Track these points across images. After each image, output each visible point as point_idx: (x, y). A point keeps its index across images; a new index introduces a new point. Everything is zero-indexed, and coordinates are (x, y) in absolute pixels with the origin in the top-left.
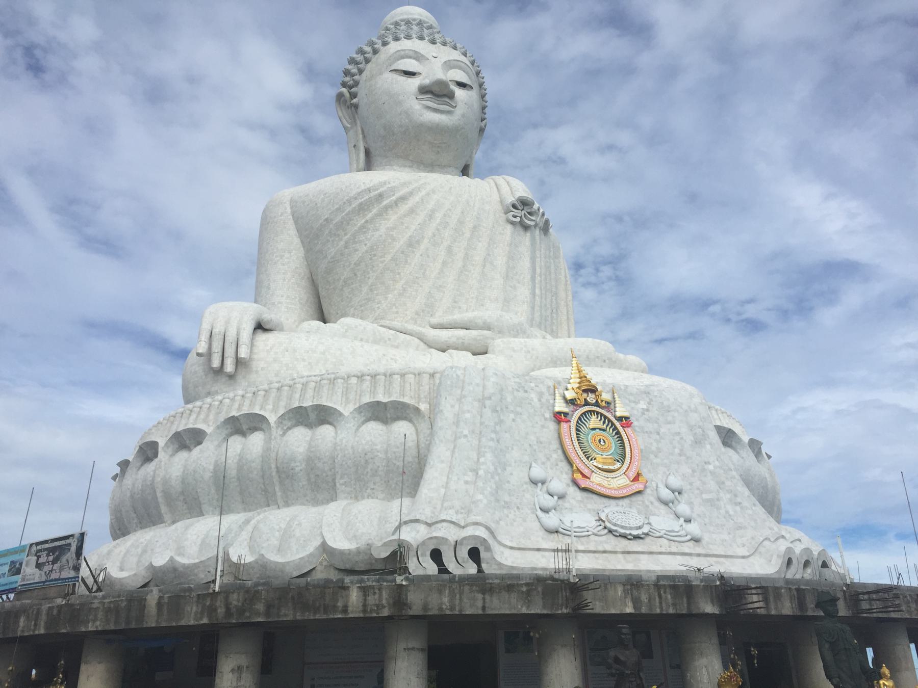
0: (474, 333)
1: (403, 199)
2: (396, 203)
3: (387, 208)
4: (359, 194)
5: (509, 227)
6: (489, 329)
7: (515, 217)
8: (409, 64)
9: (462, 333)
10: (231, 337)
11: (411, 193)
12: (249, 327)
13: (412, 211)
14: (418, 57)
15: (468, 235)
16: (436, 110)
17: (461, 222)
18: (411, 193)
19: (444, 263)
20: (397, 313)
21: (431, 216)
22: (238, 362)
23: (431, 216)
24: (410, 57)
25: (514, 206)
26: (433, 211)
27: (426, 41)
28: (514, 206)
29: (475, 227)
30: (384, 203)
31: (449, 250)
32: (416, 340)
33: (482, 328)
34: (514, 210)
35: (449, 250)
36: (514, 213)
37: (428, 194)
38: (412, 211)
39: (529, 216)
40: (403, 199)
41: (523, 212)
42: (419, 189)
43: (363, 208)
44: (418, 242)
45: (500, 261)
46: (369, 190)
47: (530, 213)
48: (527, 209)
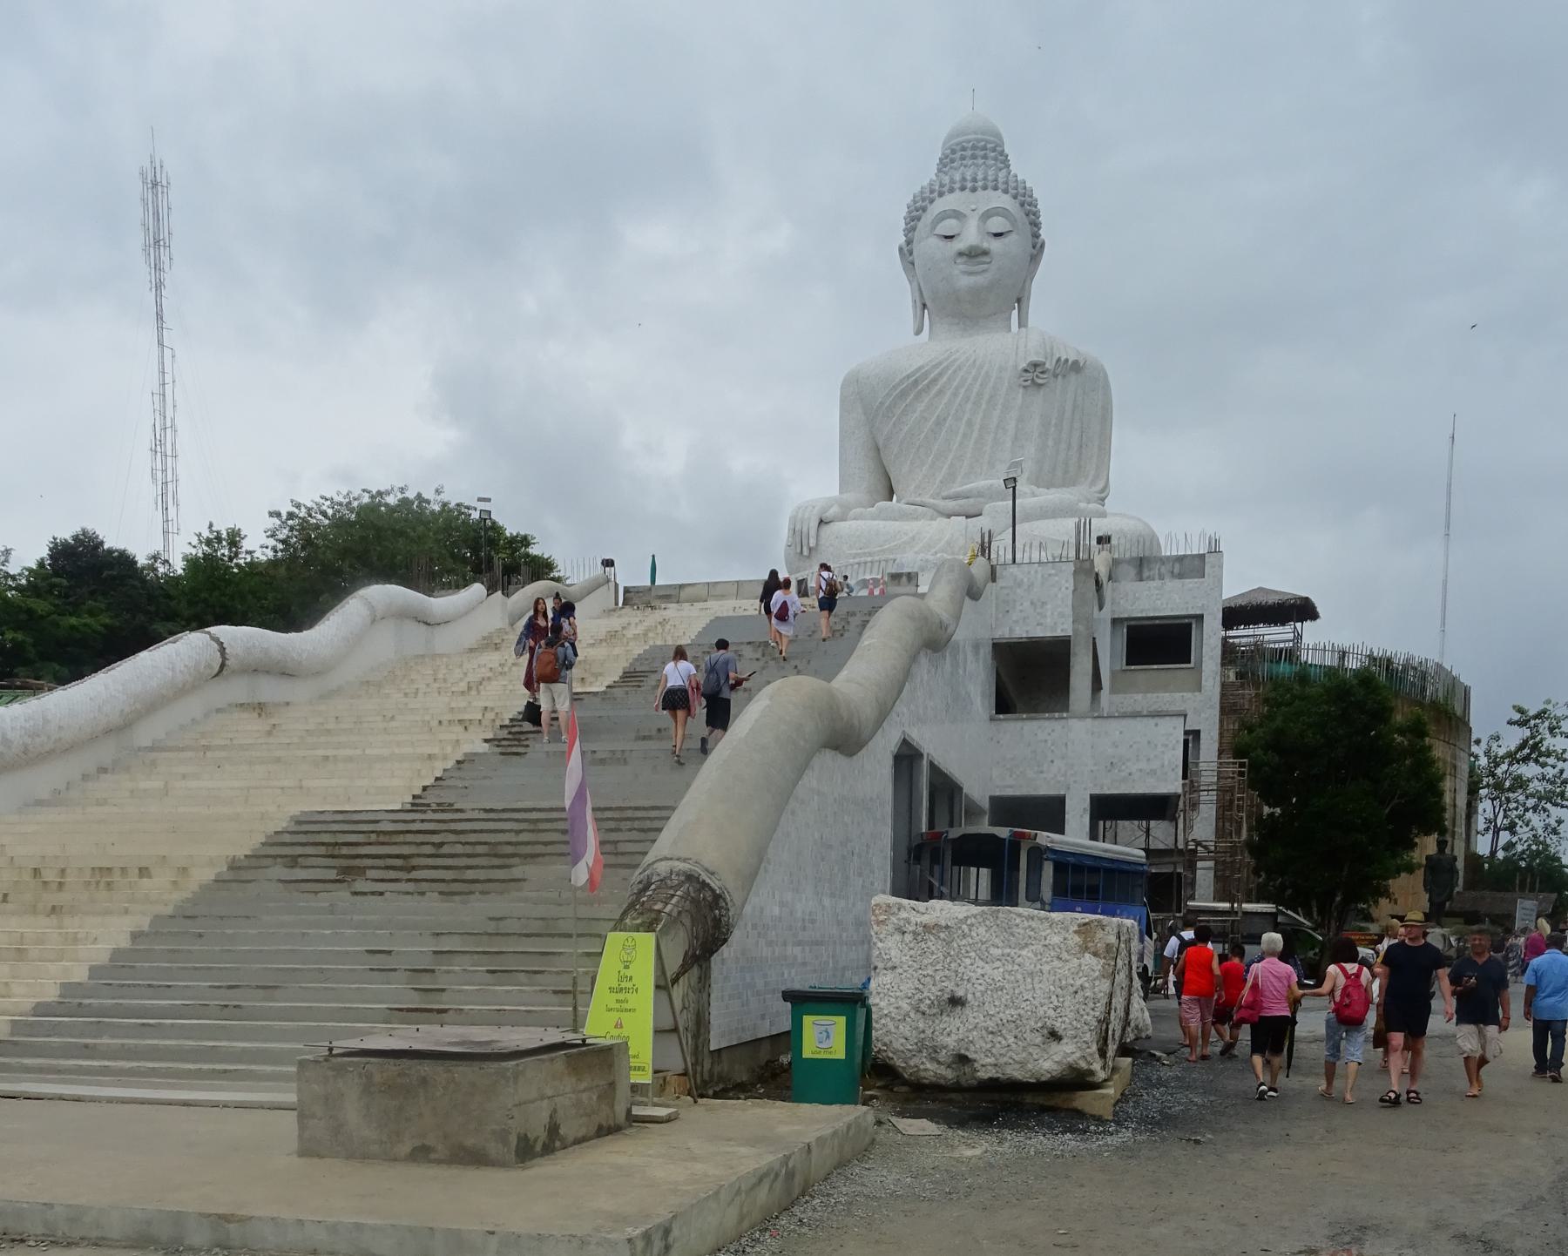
0: (972, 500)
1: (935, 380)
2: (928, 387)
3: (923, 390)
4: (901, 381)
5: (1021, 390)
6: (982, 496)
7: (1026, 381)
8: (949, 226)
9: (962, 502)
10: (805, 530)
11: (940, 374)
12: (814, 524)
13: (940, 392)
14: (957, 215)
15: (984, 406)
16: (970, 273)
17: (980, 394)
18: (940, 374)
19: (965, 435)
20: (929, 482)
21: (955, 395)
22: (810, 549)
23: (955, 395)
24: (949, 217)
25: (1026, 371)
26: (957, 388)
27: (967, 190)
28: (1026, 371)
29: (991, 397)
30: (919, 388)
31: (970, 424)
32: (931, 510)
33: (977, 497)
34: (1025, 374)
35: (970, 424)
36: (1022, 379)
37: (955, 372)
38: (940, 392)
39: (1041, 376)
40: (935, 380)
41: (1035, 374)
42: (947, 368)
43: (903, 394)
44: (945, 419)
45: (1011, 426)
46: (908, 377)
47: (1042, 373)
48: (1039, 369)
